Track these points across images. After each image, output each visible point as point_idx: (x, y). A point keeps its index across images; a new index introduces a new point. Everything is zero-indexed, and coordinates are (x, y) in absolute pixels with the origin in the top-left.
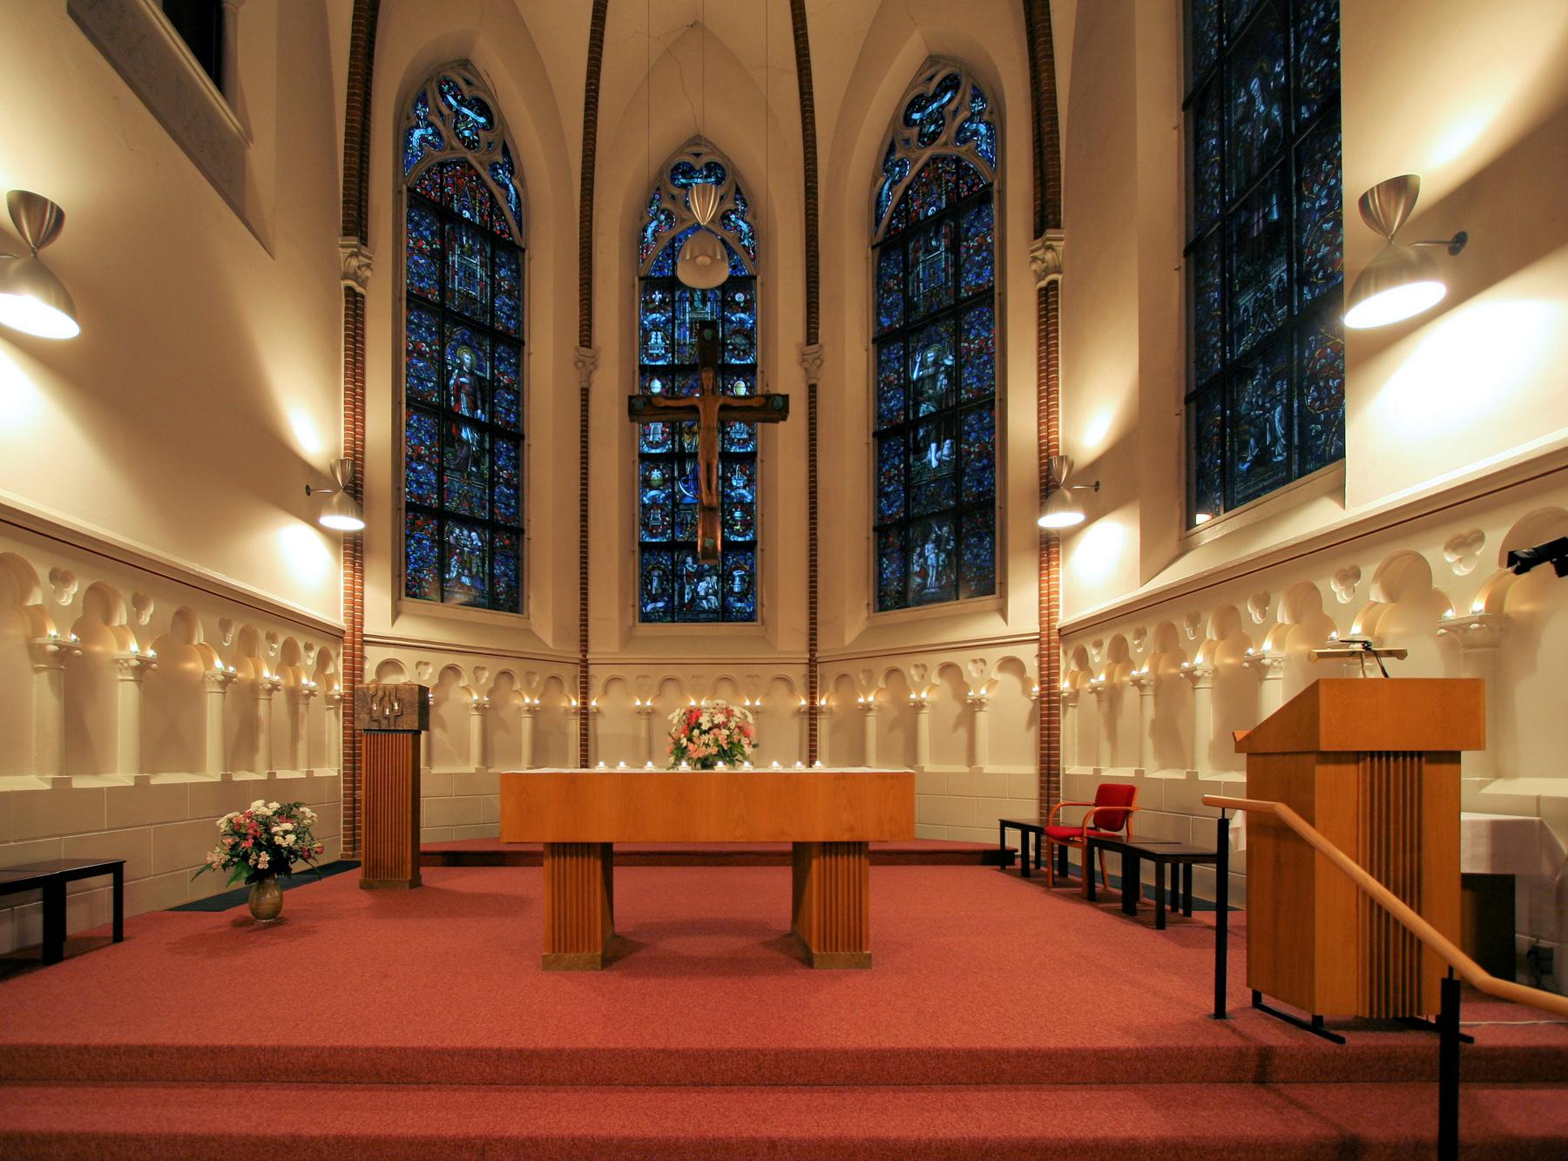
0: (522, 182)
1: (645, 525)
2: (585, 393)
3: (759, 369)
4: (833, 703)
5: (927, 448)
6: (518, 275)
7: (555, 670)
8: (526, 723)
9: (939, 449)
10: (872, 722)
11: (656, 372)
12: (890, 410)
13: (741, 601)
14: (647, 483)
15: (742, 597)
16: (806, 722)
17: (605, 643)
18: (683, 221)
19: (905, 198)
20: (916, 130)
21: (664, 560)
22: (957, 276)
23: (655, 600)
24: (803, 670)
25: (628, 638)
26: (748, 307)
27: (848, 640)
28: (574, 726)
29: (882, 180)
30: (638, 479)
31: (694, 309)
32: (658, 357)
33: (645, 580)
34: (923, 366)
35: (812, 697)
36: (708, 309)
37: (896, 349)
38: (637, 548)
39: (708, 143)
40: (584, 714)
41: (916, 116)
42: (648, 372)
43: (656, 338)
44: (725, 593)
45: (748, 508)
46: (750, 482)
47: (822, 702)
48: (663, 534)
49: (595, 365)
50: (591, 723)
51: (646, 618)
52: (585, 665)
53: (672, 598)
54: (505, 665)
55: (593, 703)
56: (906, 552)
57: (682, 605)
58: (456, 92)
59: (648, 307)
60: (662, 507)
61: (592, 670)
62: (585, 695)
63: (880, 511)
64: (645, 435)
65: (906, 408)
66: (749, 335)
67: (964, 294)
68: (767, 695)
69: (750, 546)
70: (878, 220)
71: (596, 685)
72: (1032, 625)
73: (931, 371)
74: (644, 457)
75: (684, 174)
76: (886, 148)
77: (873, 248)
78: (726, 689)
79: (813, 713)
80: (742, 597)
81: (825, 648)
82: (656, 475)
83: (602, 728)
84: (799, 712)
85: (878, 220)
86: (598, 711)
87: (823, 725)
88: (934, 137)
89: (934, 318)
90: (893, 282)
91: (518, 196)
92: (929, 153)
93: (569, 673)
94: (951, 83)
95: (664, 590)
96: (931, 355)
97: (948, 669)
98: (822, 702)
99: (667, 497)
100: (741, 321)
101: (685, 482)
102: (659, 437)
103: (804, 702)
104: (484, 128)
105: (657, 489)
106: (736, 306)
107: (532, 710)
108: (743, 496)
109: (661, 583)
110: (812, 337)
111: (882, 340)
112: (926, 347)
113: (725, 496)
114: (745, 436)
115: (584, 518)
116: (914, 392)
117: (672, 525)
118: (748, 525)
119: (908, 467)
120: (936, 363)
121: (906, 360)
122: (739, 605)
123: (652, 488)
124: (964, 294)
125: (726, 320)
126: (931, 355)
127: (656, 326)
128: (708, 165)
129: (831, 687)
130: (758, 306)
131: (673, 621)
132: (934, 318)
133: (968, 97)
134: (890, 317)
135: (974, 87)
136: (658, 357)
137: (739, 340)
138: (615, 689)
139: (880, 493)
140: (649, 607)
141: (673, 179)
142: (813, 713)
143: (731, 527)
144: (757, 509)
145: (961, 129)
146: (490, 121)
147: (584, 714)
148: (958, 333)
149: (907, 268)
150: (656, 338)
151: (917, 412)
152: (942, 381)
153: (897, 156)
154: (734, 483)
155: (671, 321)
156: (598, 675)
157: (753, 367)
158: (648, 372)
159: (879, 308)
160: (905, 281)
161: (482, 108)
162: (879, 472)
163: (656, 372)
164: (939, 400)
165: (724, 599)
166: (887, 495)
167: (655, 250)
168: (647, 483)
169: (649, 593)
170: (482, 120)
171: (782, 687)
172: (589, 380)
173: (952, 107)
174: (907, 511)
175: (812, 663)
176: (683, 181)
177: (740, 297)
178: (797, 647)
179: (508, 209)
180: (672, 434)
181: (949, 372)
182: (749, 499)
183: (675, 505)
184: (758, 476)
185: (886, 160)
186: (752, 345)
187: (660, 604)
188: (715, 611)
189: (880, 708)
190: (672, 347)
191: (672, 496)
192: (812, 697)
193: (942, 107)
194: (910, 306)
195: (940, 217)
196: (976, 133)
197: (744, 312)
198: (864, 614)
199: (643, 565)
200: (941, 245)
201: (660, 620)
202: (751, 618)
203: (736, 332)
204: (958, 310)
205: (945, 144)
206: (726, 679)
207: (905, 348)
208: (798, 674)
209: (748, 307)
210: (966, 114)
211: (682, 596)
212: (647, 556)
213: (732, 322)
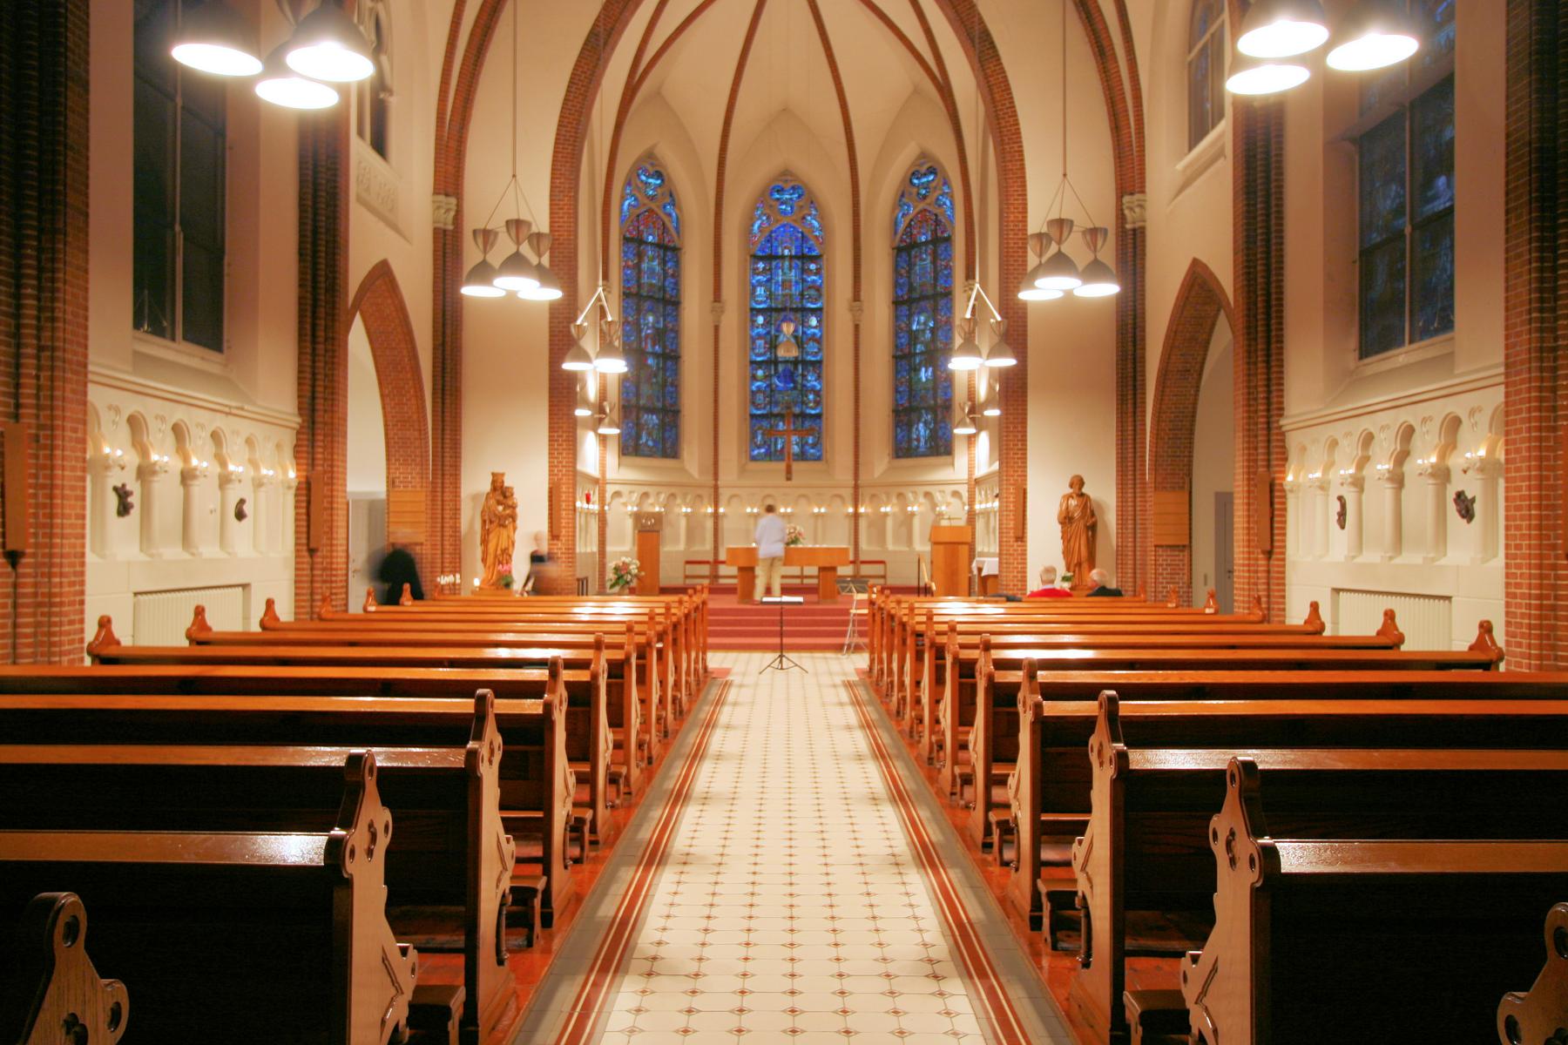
0: (681, 210)
1: (753, 403)
2: (717, 329)
3: (825, 310)
4: (869, 510)
5: (920, 370)
6: (677, 264)
7: (700, 491)
8: (683, 523)
9: (926, 371)
10: (889, 523)
11: (760, 311)
12: (902, 344)
13: (813, 448)
14: (754, 378)
15: (814, 446)
16: (853, 522)
17: (728, 473)
18: (778, 221)
19: (909, 225)
20: (914, 190)
21: (765, 423)
22: (936, 279)
23: (759, 447)
24: (850, 491)
25: (742, 471)
26: (818, 272)
27: (876, 476)
28: (710, 524)
29: (897, 211)
30: (749, 375)
31: (784, 274)
32: (761, 303)
33: (753, 435)
34: (918, 323)
35: (856, 506)
36: (793, 273)
37: (905, 308)
38: (748, 417)
39: (792, 174)
40: (716, 515)
41: (916, 181)
42: (755, 312)
43: (760, 291)
44: (803, 445)
45: (817, 393)
46: (819, 378)
47: (862, 510)
48: (764, 408)
49: (722, 312)
50: (720, 522)
51: (753, 459)
52: (716, 488)
53: (769, 446)
54: (673, 490)
55: (721, 510)
56: (910, 425)
57: (776, 451)
58: (645, 171)
59: (755, 272)
60: (764, 393)
61: (721, 490)
62: (716, 506)
63: (896, 400)
64: (753, 349)
65: (909, 344)
66: (818, 289)
67: (939, 289)
68: (829, 506)
69: (819, 416)
70: (896, 233)
71: (723, 497)
72: (964, 476)
73: (922, 327)
74: (752, 362)
75: (778, 191)
76: (900, 193)
77: (893, 249)
78: (803, 501)
79: (856, 516)
80: (814, 446)
81: (863, 479)
82: (760, 373)
83: (726, 525)
84: (848, 515)
85: (896, 233)
86: (724, 515)
87: (863, 523)
88: (925, 197)
89: (924, 298)
90: (903, 271)
91: (677, 218)
92: (921, 206)
93: (707, 493)
94: (932, 171)
95: (765, 442)
96: (922, 319)
97: (927, 495)
98: (862, 510)
99: (767, 386)
100: (814, 281)
101: (778, 377)
102: (762, 351)
103: (851, 510)
104: (660, 186)
105: (761, 381)
106: (810, 272)
107: (687, 515)
108: (814, 386)
109: (762, 438)
110: (856, 296)
111: (897, 303)
112: (919, 313)
113: (803, 386)
114: (816, 350)
115: (716, 401)
116: (914, 337)
117: (770, 403)
118: (818, 403)
119: (910, 378)
120: (925, 323)
121: (910, 317)
122: (812, 451)
123: (757, 381)
124: (939, 289)
125: (804, 281)
126: (922, 319)
127: (760, 284)
128: (793, 188)
129: (867, 500)
130: (824, 272)
131: (771, 460)
132: (924, 298)
133: (941, 183)
134: (902, 290)
135: (944, 179)
136: (761, 303)
137: (813, 292)
138: (735, 500)
139: (897, 391)
140: (756, 452)
141: (771, 194)
142: (856, 516)
143: (806, 404)
144: (823, 393)
145: (938, 199)
146: (663, 180)
147: (716, 515)
148: (935, 310)
149: (911, 265)
150: (760, 291)
151: (915, 349)
152: (928, 335)
153: (905, 200)
154: (809, 378)
155: (769, 280)
156: (724, 494)
157: (820, 309)
158: (755, 312)
159: (896, 285)
160: (909, 272)
161: (659, 175)
162: (896, 378)
163: (760, 311)
164: (926, 344)
165: (803, 446)
166: (900, 392)
167: (759, 238)
168: (754, 378)
169: (755, 443)
170: (659, 182)
171: (838, 501)
172: (719, 321)
173: (933, 184)
174: (910, 403)
175: (856, 487)
176: (778, 196)
177: (813, 267)
178: (844, 475)
179: (671, 226)
180: (770, 348)
181: (933, 331)
182: (818, 387)
183: (772, 391)
184: (824, 374)
185: (900, 200)
186: (820, 296)
187: (763, 450)
188: (797, 455)
189: (894, 514)
190: (770, 297)
191: (769, 386)
192: (856, 506)
193: (929, 182)
194: (911, 289)
195: (926, 243)
196: (945, 204)
197: (816, 274)
198: (886, 459)
199: (752, 427)
200: (928, 260)
201: (762, 460)
202: (819, 459)
203: (810, 288)
204: (935, 297)
205: (930, 204)
206: (804, 496)
207: (909, 310)
208: (848, 493)
209: (818, 272)
210: (940, 192)
211: (776, 445)
212: (754, 421)
213: (807, 282)
